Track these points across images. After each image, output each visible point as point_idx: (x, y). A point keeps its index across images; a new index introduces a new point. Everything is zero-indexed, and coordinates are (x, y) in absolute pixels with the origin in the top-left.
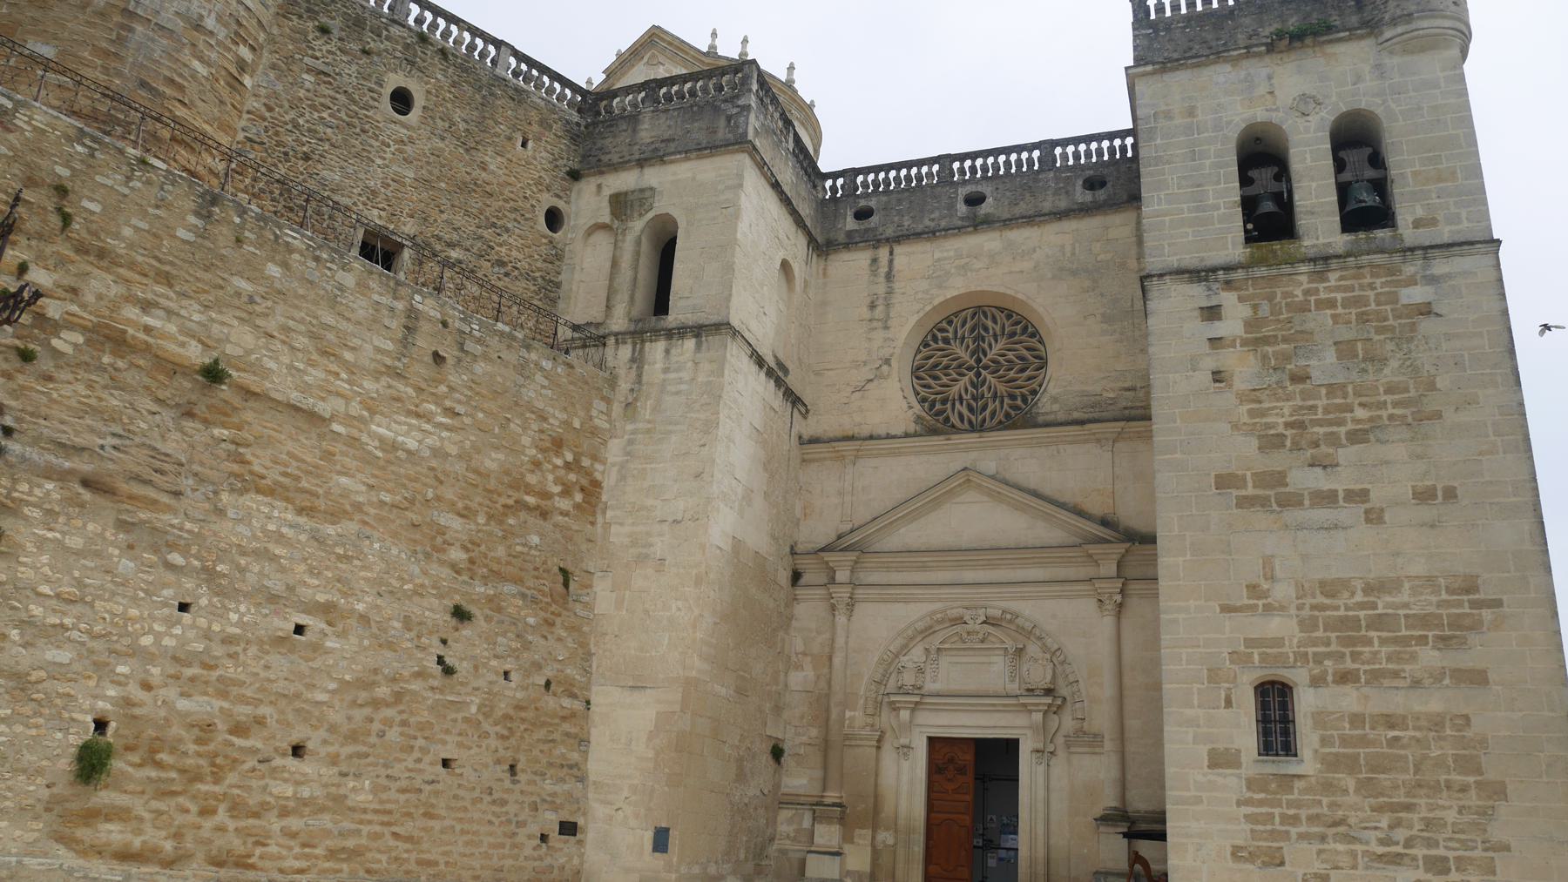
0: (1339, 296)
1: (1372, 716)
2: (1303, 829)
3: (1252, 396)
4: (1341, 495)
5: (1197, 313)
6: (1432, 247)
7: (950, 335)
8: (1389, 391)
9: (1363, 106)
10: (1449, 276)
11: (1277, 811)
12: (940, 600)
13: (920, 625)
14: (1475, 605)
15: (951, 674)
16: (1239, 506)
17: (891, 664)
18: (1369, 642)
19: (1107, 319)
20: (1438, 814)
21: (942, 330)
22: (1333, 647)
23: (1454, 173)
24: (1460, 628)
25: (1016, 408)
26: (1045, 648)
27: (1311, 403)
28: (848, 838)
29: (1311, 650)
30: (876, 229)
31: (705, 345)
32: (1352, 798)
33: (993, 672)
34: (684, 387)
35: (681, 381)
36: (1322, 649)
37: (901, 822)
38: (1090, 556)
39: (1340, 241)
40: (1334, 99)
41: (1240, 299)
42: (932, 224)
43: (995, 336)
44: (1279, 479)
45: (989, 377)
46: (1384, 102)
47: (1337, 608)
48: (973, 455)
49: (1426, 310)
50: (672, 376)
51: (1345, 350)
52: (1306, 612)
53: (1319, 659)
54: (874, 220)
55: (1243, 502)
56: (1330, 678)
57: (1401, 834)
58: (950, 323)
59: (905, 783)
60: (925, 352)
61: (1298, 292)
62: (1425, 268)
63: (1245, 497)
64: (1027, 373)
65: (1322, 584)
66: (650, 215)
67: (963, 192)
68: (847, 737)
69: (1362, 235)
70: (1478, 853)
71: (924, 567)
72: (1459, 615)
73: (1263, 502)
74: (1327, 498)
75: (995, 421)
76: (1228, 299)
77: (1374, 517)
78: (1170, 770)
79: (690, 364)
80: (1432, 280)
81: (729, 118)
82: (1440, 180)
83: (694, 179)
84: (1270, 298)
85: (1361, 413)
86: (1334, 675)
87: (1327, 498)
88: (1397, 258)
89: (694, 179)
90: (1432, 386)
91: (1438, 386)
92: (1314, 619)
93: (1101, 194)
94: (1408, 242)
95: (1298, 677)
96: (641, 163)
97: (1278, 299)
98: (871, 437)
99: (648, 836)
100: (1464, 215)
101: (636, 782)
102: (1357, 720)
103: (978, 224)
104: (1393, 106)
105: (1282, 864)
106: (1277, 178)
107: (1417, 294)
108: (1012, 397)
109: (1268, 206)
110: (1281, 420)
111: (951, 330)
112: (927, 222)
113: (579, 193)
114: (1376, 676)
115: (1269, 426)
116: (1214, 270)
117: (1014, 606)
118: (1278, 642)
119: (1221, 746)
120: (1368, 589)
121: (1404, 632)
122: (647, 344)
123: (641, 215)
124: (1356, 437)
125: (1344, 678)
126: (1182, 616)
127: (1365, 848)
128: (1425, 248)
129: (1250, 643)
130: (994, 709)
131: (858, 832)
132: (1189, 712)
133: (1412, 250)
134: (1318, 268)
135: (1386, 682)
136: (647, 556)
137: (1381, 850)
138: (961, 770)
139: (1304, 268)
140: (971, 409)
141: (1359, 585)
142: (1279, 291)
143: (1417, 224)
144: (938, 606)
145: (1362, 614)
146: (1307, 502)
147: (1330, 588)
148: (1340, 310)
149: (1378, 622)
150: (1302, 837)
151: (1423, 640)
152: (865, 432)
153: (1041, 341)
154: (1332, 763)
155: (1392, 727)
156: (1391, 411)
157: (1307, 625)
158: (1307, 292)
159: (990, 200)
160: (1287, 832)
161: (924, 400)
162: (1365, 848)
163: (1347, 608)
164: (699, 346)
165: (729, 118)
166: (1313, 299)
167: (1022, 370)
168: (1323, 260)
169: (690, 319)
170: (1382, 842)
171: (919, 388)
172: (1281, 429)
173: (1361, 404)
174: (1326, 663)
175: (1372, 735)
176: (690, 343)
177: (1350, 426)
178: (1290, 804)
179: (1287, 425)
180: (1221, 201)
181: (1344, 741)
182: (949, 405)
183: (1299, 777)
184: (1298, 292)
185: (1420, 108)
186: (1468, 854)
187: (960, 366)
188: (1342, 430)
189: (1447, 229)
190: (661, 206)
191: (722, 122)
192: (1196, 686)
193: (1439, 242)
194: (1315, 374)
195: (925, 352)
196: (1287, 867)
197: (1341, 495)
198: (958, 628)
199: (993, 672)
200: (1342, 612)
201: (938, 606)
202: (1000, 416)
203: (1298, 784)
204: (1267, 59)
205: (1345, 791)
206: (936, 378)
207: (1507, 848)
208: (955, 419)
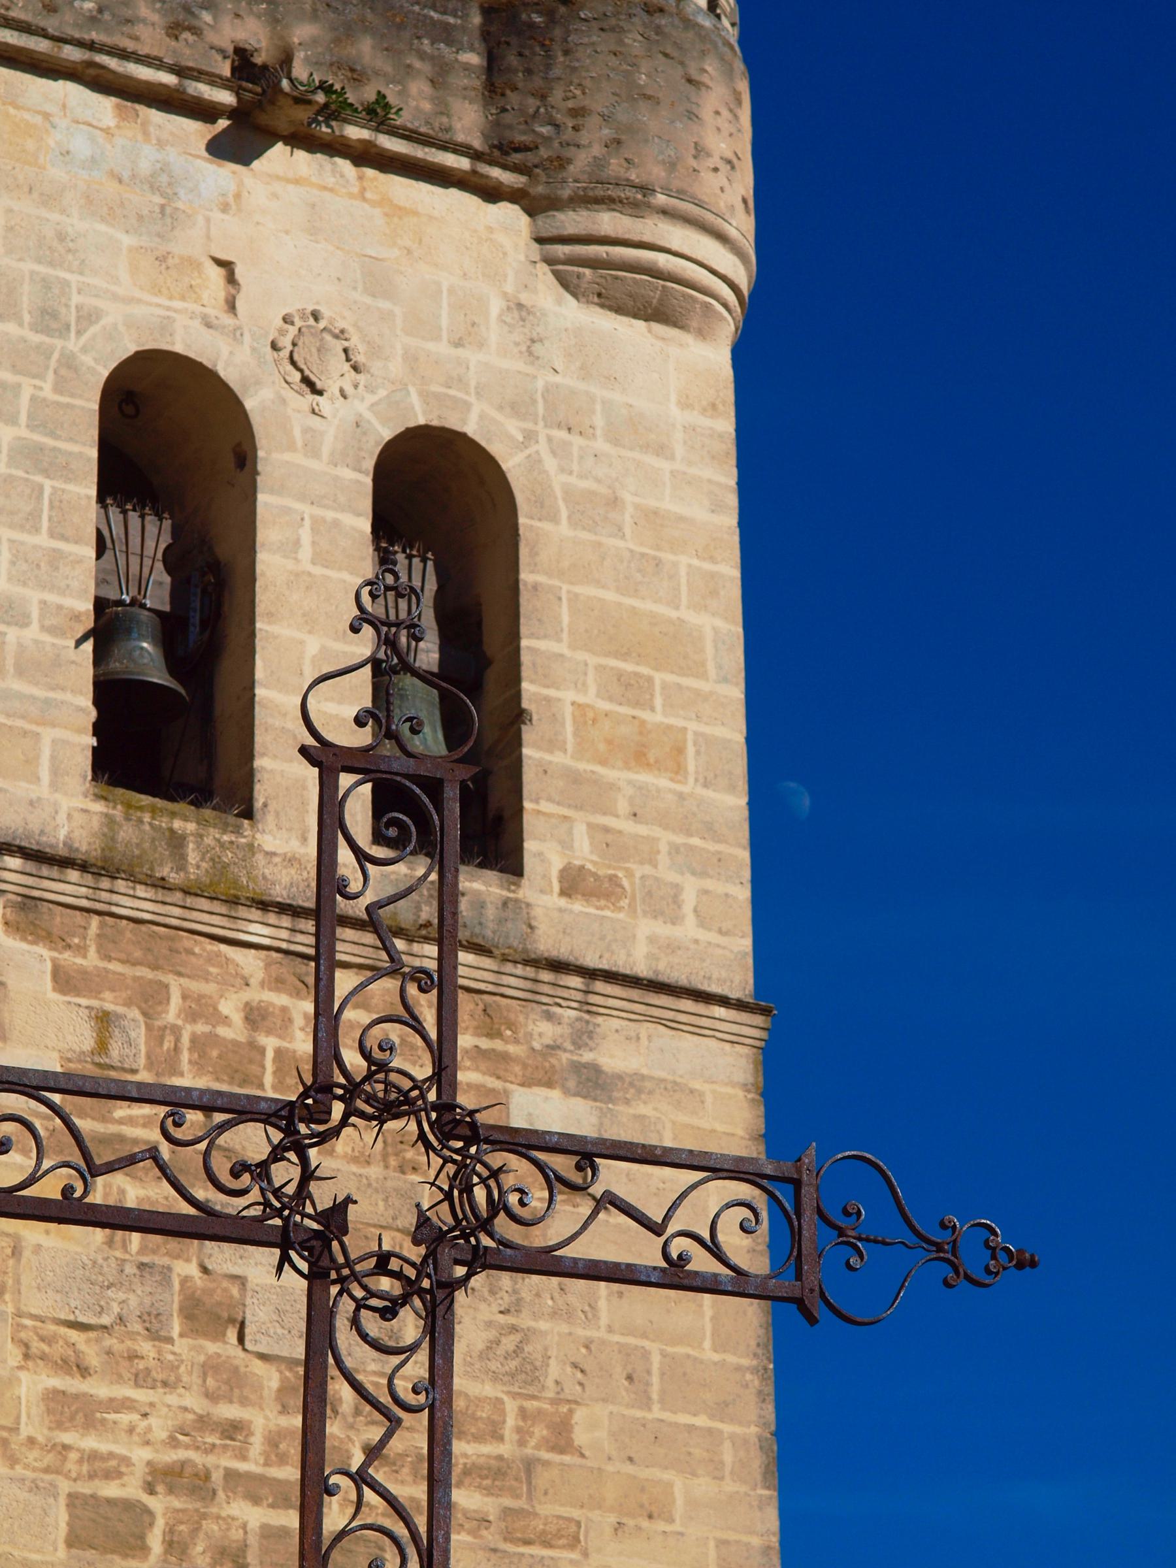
6: (611, 976)
9: (471, 429)
23: (680, 750)
27: (228, 1411)
40: (396, 368)
41: (64, 980)
46: (530, 437)
61: (230, 1006)
62: (583, 1037)
82: (639, 757)
84: (150, 999)
88: (515, 978)
90: (561, 1437)
91: (580, 1437)
94: (547, 943)
97: (172, 1014)
100: (689, 899)
104: (550, 464)
110: (141, 1455)
115: (107, 1467)
133: (559, 966)
139: (258, 930)
142: (176, 986)
143: (573, 883)
158: (255, 1017)
166: (270, 1043)
172: (129, 1489)
179: (164, 1477)
180: (33, 597)
184: (230, 1006)
185: (614, 502)
189: (646, 927)
193: (620, 962)
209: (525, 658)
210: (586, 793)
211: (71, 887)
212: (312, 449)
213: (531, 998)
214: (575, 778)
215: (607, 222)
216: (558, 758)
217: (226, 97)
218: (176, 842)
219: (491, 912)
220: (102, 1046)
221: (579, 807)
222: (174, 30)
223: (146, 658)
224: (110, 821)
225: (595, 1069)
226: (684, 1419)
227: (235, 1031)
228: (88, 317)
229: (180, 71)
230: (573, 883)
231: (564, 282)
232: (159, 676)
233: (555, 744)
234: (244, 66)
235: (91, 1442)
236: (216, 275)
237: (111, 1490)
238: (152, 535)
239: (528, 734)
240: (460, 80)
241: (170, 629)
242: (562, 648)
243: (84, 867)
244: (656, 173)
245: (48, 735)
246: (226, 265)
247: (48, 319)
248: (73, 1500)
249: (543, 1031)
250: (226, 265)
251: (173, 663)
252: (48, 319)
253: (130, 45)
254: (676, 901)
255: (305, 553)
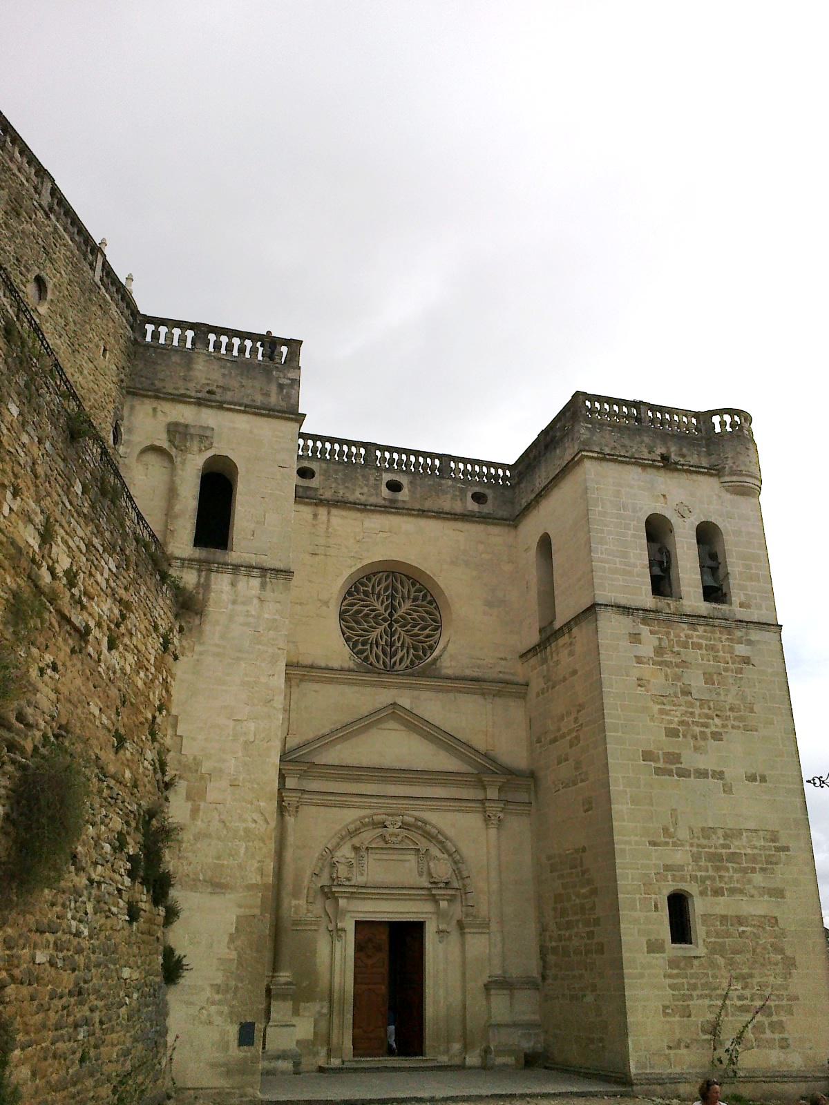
0: (704, 642)
1: (732, 916)
2: (698, 992)
3: (661, 698)
4: (710, 773)
5: (627, 636)
6: (751, 622)
7: (370, 590)
8: (731, 709)
9: (712, 520)
10: (758, 641)
11: (685, 980)
12: (370, 807)
13: (352, 827)
14: (778, 849)
15: (376, 870)
16: (657, 774)
17: (329, 860)
18: (727, 869)
19: (489, 604)
20: (764, 979)
21: (363, 584)
22: (711, 873)
24: (771, 863)
25: (420, 658)
26: (444, 849)
27: (691, 710)
28: (296, 1012)
29: (699, 874)
30: (316, 490)
31: (269, 586)
32: (724, 972)
33: (406, 870)
34: (251, 620)
35: (248, 614)
36: (703, 874)
37: (336, 996)
38: (482, 782)
39: (704, 607)
41: (651, 632)
42: (363, 498)
43: (403, 597)
44: (674, 758)
45: (399, 629)
46: (724, 521)
47: (710, 847)
48: (394, 692)
49: (746, 660)
50: (239, 608)
51: (709, 679)
52: (695, 849)
53: (703, 880)
54: (314, 483)
55: (658, 771)
56: (709, 893)
57: (747, 993)
58: (369, 579)
59: (336, 960)
60: (349, 600)
62: (747, 634)
63: (659, 768)
64: (427, 631)
65: (703, 829)
66: (210, 453)
67: (387, 477)
68: (296, 923)
69: (714, 605)
70: (784, 1002)
71: (358, 779)
72: (770, 855)
73: (669, 773)
74: (702, 774)
75: (403, 665)
76: (644, 630)
77: (728, 789)
78: (625, 955)
79: (255, 601)
80: (749, 642)
81: (281, 387)
82: (751, 579)
83: (251, 432)
84: (668, 634)
85: (716, 720)
86: (712, 889)
87: (702, 774)
89: (251, 432)
90: (752, 711)
91: (755, 710)
92: (699, 853)
93: (487, 508)
94: (739, 617)
95: (692, 888)
96: (200, 403)
97: (672, 636)
98: (312, 667)
99: (233, 1031)
100: (764, 606)
101: (218, 981)
102: (724, 919)
103: (391, 508)
105: (689, 1016)
106: (660, 551)
107: (741, 650)
108: (416, 649)
109: (657, 571)
110: (676, 719)
111: (371, 586)
112: (357, 494)
113: (132, 408)
114: (733, 891)
115: (671, 722)
116: (637, 609)
117: (427, 816)
118: (681, 868)
119: (652, 938)
120: (726, 836)
121: (745, 865)
122: (213, 575)
123: (200, 450)
124: (717, 736)
125: (717, 892)
126: (627, 847)
127: (732, 1002)
128: (747, 622)
129: (667, 868)
130: (410, 898)
131: (302, 1005)
132: (636, 914)
133: (741, 621)
134: (694, 621)
135: (738, 897)
136: (221, 771)
137: (739, 1003)
138: (378, 949)
140: (384, 653)
141: (720, 832)
144: (368, 812)
145: (724, 851)
146: (692, 776)
147: (707, 832)
148: (704, 652)
149: (733, 857)
150: (700, 997)
151: (753, 870)
152: (308, 661)
153: (437, 608)
154: (715, 949)
155: (741, 924)
156: (732, 722)
157: (696, 858)
159: (405, 490)
160: (692, 995)
161: (347, 640)
162: (732, 1002)
163: (716, 848)
164: (263, 586)
165: (281, 387)
166: (690, 641)
167: (423, 629)
168: (695, 619)
169: (253, 559)
170: (741, 998)
171: (343, 627)
173: (717, 715)
174: (708, 882)
175: (731, 929)
176: (256, 582)
177: (714, 729)
178: (692, 976)
179: (682, 723)
181: (718, 935)
182: (368, 647)
183: (696, 957)
184: (682, 635)
186: (780, 1003)
187: (376, 617)
188: (708, 731)
190: (221, 448)
191: (274, 389)
192: (638, 896)
194: (693, 692)
195: (349, 600)
196: (693, 1018)
197: (710, 773)
198: (379, 831)
199: (406, 870)
200: (712, 850)
201: (368, 812)
202: (407, 662)
203: (696, 962)
204: (662, 471)
205: (719, 968)
206: (357, 622)
207: (797, 998)
208: (372, 659)
209: (728, 563)
210: (742, 588)
211: (651, 615)
212: (684, 529)
213: (737, 628)
214: (739, 585)
215: (735, 478)
216: (737, 582)
217: (662, 464)
218: (669, 604)
219: (727, 612)
220: (660, 644)
221: (741, 590)
222: (649, 453)
223: (657, 571)
224: (657, 602)
225: (750, 640)
226: (775, 705)
227: (683, 639)
228: (641, 509)
229: (652, 460)
230: (742, 605)
231: (727, 490)
232: (660, 573)
233: (735, 579)
234: (662, 456)
235: (668, 718)
236: (662, 497)
237: (672, 726)
238: (656, 546)
239: (730, 577)
240: (702, 454)
241: (661, 563)
242: (734, 560)
243: (653, 611)
244: (743, 468)
245: (644, 587)
246: (664, 496)
247: (634, 511)
248: (665, 728)
249: (738, 634)
250: (664, 496)
251: (662, 570)
252: (634, 511)
253: (642, 457)
254: (761, 606)
255: (685, 549)
